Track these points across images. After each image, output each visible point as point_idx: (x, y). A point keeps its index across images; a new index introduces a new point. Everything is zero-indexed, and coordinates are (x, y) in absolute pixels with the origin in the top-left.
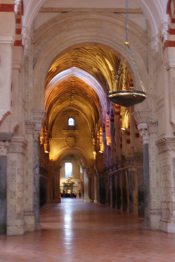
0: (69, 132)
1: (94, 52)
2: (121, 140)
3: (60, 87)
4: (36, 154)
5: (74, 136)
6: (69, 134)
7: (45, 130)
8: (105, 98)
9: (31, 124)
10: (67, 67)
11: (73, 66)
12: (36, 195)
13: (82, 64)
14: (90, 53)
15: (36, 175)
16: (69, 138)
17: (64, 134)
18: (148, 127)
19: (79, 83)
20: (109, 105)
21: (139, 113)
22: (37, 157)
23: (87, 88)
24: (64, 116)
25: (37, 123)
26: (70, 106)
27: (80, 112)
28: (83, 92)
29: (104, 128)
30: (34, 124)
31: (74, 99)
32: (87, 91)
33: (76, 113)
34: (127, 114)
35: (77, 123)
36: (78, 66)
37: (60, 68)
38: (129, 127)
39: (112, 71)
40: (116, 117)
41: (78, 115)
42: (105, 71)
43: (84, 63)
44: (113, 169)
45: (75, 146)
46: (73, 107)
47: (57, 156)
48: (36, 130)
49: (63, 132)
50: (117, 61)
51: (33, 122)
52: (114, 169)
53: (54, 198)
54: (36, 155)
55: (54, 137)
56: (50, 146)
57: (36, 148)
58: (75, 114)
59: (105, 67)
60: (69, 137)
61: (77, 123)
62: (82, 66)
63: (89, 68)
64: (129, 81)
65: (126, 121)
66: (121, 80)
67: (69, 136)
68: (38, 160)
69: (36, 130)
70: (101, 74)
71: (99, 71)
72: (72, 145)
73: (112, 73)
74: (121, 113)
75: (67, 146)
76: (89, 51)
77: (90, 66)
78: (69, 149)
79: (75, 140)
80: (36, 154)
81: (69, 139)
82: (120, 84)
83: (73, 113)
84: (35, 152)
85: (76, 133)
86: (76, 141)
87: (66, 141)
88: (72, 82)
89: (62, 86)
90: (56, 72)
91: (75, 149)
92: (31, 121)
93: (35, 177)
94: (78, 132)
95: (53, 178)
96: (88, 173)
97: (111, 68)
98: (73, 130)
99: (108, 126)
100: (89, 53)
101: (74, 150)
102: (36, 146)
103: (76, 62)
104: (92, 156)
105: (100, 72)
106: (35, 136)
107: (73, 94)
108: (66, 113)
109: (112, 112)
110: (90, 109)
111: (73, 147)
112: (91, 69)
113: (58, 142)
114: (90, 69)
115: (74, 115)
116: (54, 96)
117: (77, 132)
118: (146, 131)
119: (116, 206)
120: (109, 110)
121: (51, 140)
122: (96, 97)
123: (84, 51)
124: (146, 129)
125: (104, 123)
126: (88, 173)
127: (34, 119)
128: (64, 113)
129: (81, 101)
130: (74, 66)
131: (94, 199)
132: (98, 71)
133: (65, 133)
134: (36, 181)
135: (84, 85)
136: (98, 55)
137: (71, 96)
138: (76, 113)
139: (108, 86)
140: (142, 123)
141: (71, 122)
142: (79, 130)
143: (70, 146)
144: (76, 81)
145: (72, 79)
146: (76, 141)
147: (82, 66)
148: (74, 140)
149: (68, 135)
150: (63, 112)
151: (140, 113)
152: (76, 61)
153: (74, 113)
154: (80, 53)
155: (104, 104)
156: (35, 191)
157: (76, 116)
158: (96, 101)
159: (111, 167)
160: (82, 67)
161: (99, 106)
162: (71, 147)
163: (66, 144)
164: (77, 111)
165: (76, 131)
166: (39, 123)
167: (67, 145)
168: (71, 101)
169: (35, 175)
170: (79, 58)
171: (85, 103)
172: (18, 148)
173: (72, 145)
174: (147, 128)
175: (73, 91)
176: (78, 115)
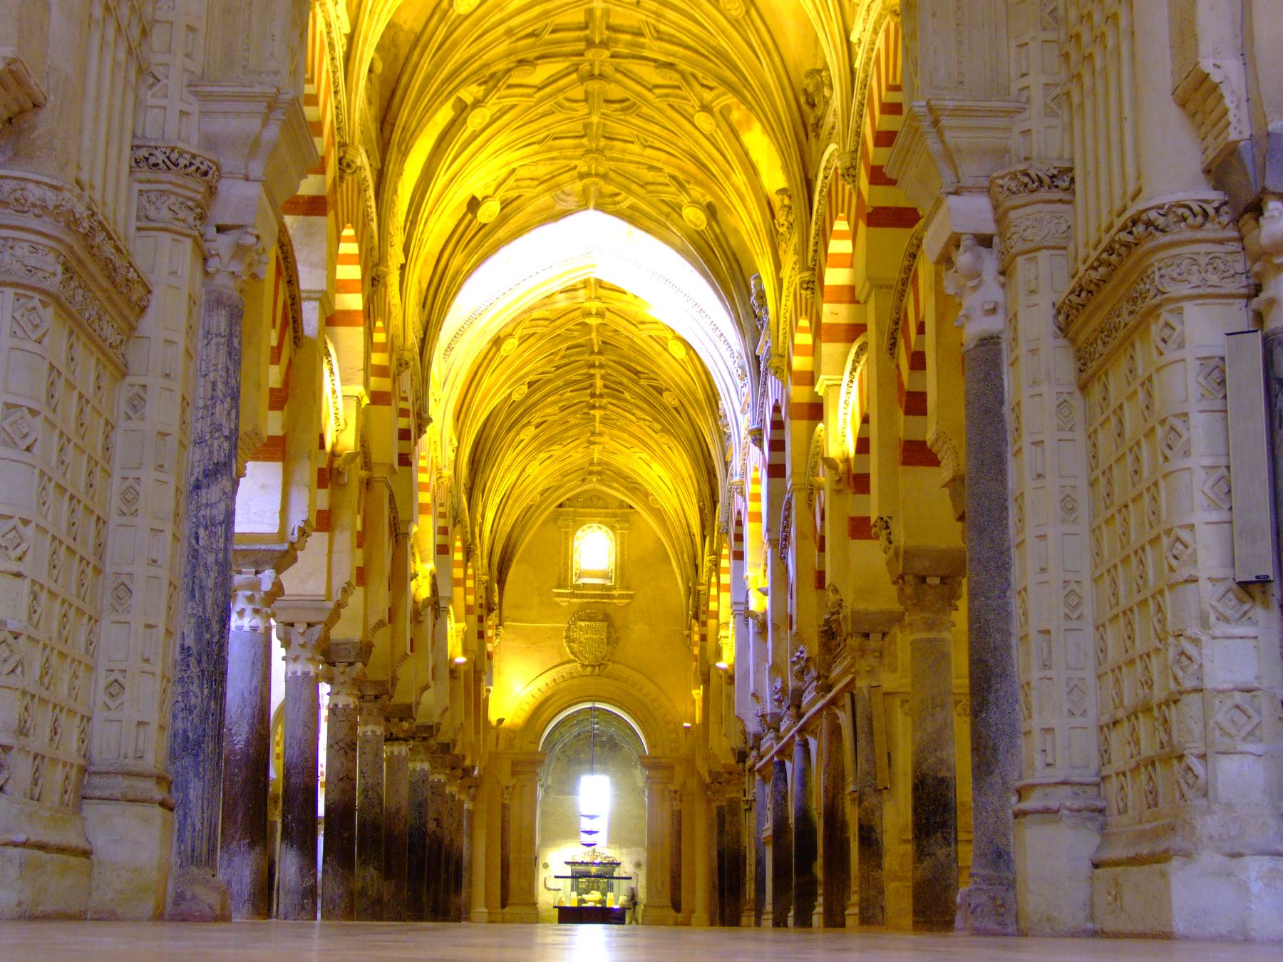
1: (685, 99)
2: (822, 548)
3: (532, 340)
4: (220, 386)
6: (583, 607)
7: (458, 556)
8: (742, 379)
9: (182, 162)
10: (558, 208)
11: (585, 207)
12: (194, 670)
13: (629, 191)
14: (664, 106)
15: (206, 528)
16: (583, 624)
17: (560, 606)
18: (1000, 219)
19: (625, 323)
20: (762, 395)
21: (936, 123)
22: (227, 406)
23: (659, 348)
25: (231, 175)
26: (591, 473)
27: (638, 508)
28: (643, 382)
29: (739, 538)
30: (206, 174)
31: (606, 430)
32: (659, 367)
33: (619, 511)
34: (856, 361)
36: (611, 207)
37: (519, 209)
38: (863, 445)
39: (782, 191)
40: (794, 430)
41: (625, 519)
42: (742, 199)
43: (642, 186)
44: (777, 730)
45: (610, 664)
46: (601, 481)
48: (220, 229)
49: (559, 595)
50: (802, 100)
51: (194, 151)
52: (782, 729)
53: (504, 905)
54: (219, 394)
55: (514, 620)
56: (496, 658)
57: (224, 350)
59: (740, 178)
60: (581, 620)
62: (631, 200)
63: (666, 209)
64: (865, 155)
65: (849, 417)
66: (822, 191)
68: (227, 432)
69: (220, 229)
70: (721, 238)
71: (714, 223)
72: (596, 657)
73: (777, 201)
74: (822, 377)
75: (575, 661)
76: (657, 91)
77: (667, 198)
78: (581, 676)
80: (214, 384)
81: (581, 627)
82: (816, 224)
84: (212, 375)
85: (616, 601)
86: (612, 641)
87: (567, 637)
88: (589, 314)
89: (543, 336)
90: (501, 233)
92: (181, 145)
93: (201, 543)
94: (621, 597)
95: (505, 807)
97: (774, 178)
99: (756, 517)
100: (657, 102)
102: (219, 335)
103: (597, 175)
104: (690, 709)
105: (717, 230)
106: (213, 264)
107: (601, 396)
108: (572, 509)
109: (778, 425)
110: (677, 474)
111: (599, 666)
112: (675, 215)
113: (532, 641)
114: (668, 215)
115: (607, 519)
116: (501, 387)
118: (984, 251)
119: (792, 913)
120: (762, 420)
121: (501, 630)
122: (701, 396)
123: (639, 95)
124: (985, 241)
125: (739, 513)
127: (211, 142)
128: (560, 509)
129: (638, 438)
130: (592, 204)
132: (709, 224)
133: (564, 602)
134: (206, 565)
135: (644, 335)
136: (706, 108)
137: (592, 412)
139: (762, 296)
140: (956, 193)
142: (628, 589)
144: (608, 314)
145: (589, 299)
146: (612, 641)
147: (631, 207)
148: (604, 635)
151: (944, 121)
152: (602, 170)
153: (610, 511)
154: (616, 110)
155: (738, 409)
156: (190, 642)
158: (703, 413)
159: (768, 718)
160: (630, 212)
161: (716, 437)
162: (593, 666)
163: (568, 650)
164: (622, 505)
166: (247, 179)
167: (573, 657)
168: (594, 443)
169: (202, 532)
170: (612, 148)
171: (651, 443)
172: (22, 250)
174: (989, 228)
175: (599, 383)
176: (625, 519)
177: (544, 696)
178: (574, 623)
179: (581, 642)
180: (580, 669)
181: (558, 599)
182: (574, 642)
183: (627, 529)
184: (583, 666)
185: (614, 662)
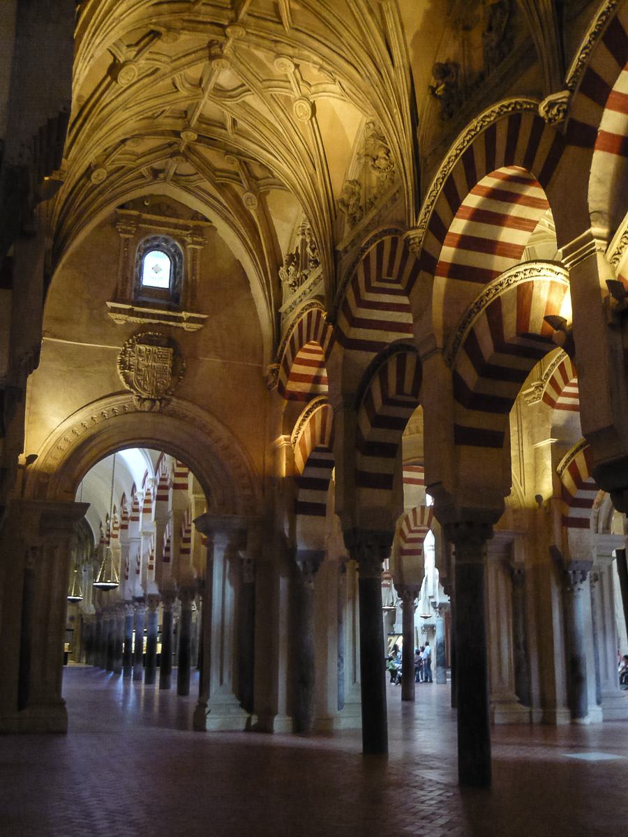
0: (143, 315)
5: (167, 339)
6: (143, 328)
16: (142, 347)
17: (114, 325)
24: (125, 232)
35: (194, 274)
45: (174, 400)
47: (64, 445)
49: (114, 310)
53: (21, 705)
58: (186, 228)
60: (140, 343)
61: (194, 274)
67: (143, 335)
72: (157, 391)
78: (137, 411)
79: (174, 361)
81: (140, 350)
83: (173, 220)
85: (184, 325)
87: (122, 362)
91: (173, 414)
95: (28, 574)
96: (241, 554)
98: (169, 309)
101: (166, 420)
108: (135, 213)
111: (160, 401)
113: (78, 365)
115: (178, 231)
117: (187, 321)
126: (241, 554)
131: (276, 713)
133: (120, 319)
138: (191, 223)
141: (156, 270)
143: (145, 395)
146: (175, 372)
148: (168, 364)
149: (135, 334)
150: (122, 207)
157: (189, 240)
162: (153, 401)
163: (121, 377)
164: (196, 215)
165: (184, 315)
167: (127, 387)
173: (157, 391)
177: (88, 434)
178: (132, 346)
179: (139, 370)
180: (135, 403)
181: (113, 316)
182: (130, 369)
183: (200, 244)
184: (141, 400)
185: (179, 398)
